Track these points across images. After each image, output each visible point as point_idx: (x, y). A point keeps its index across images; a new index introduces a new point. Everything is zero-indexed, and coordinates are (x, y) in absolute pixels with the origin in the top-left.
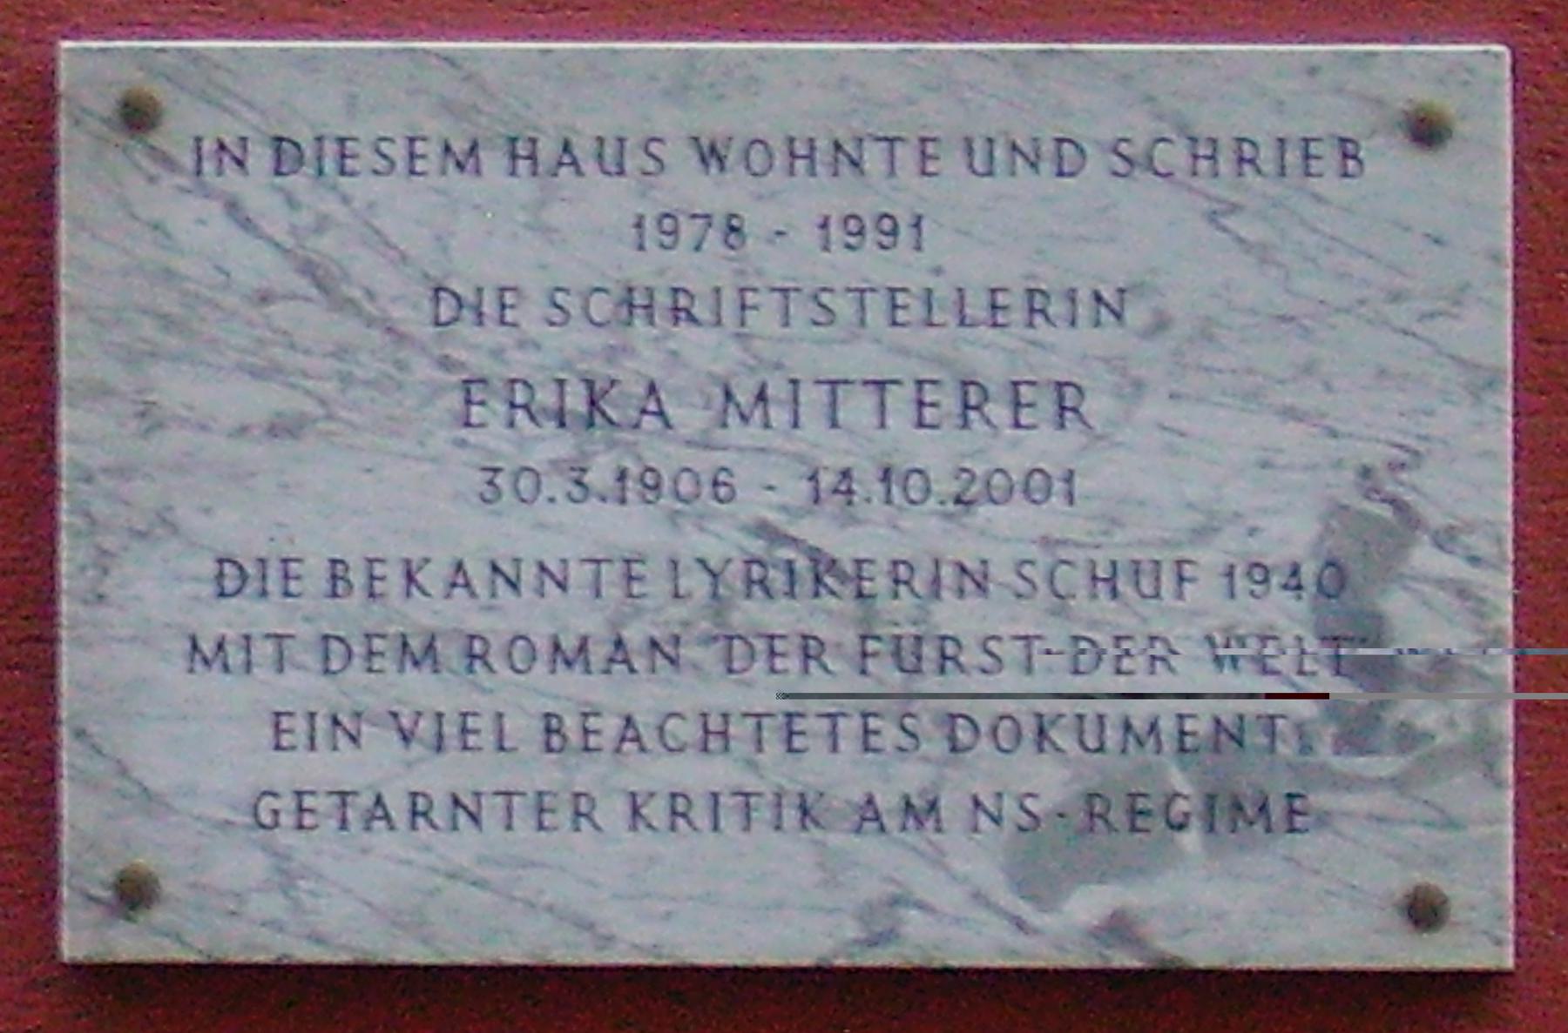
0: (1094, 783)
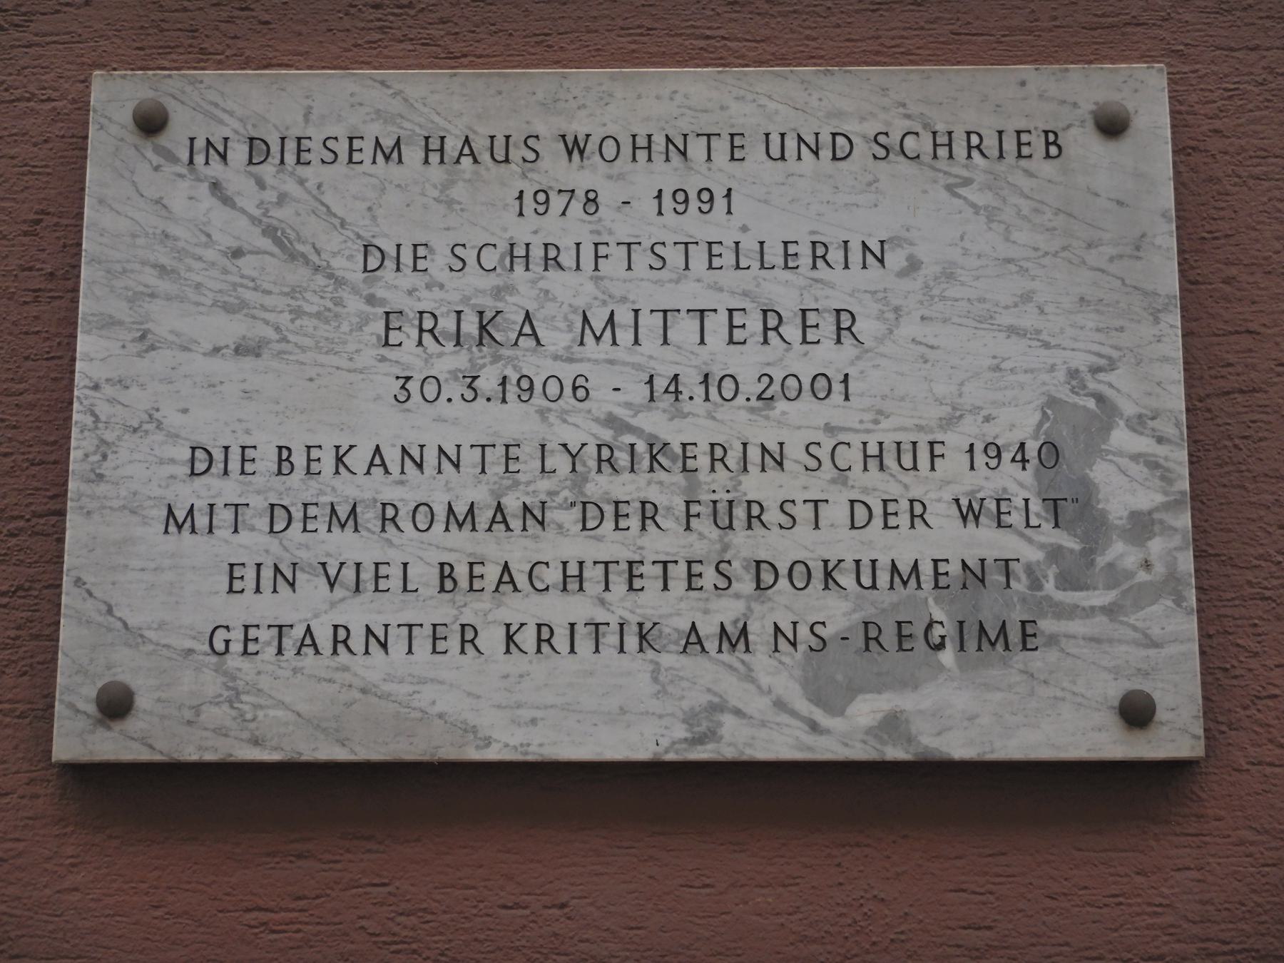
0: (868, 613)
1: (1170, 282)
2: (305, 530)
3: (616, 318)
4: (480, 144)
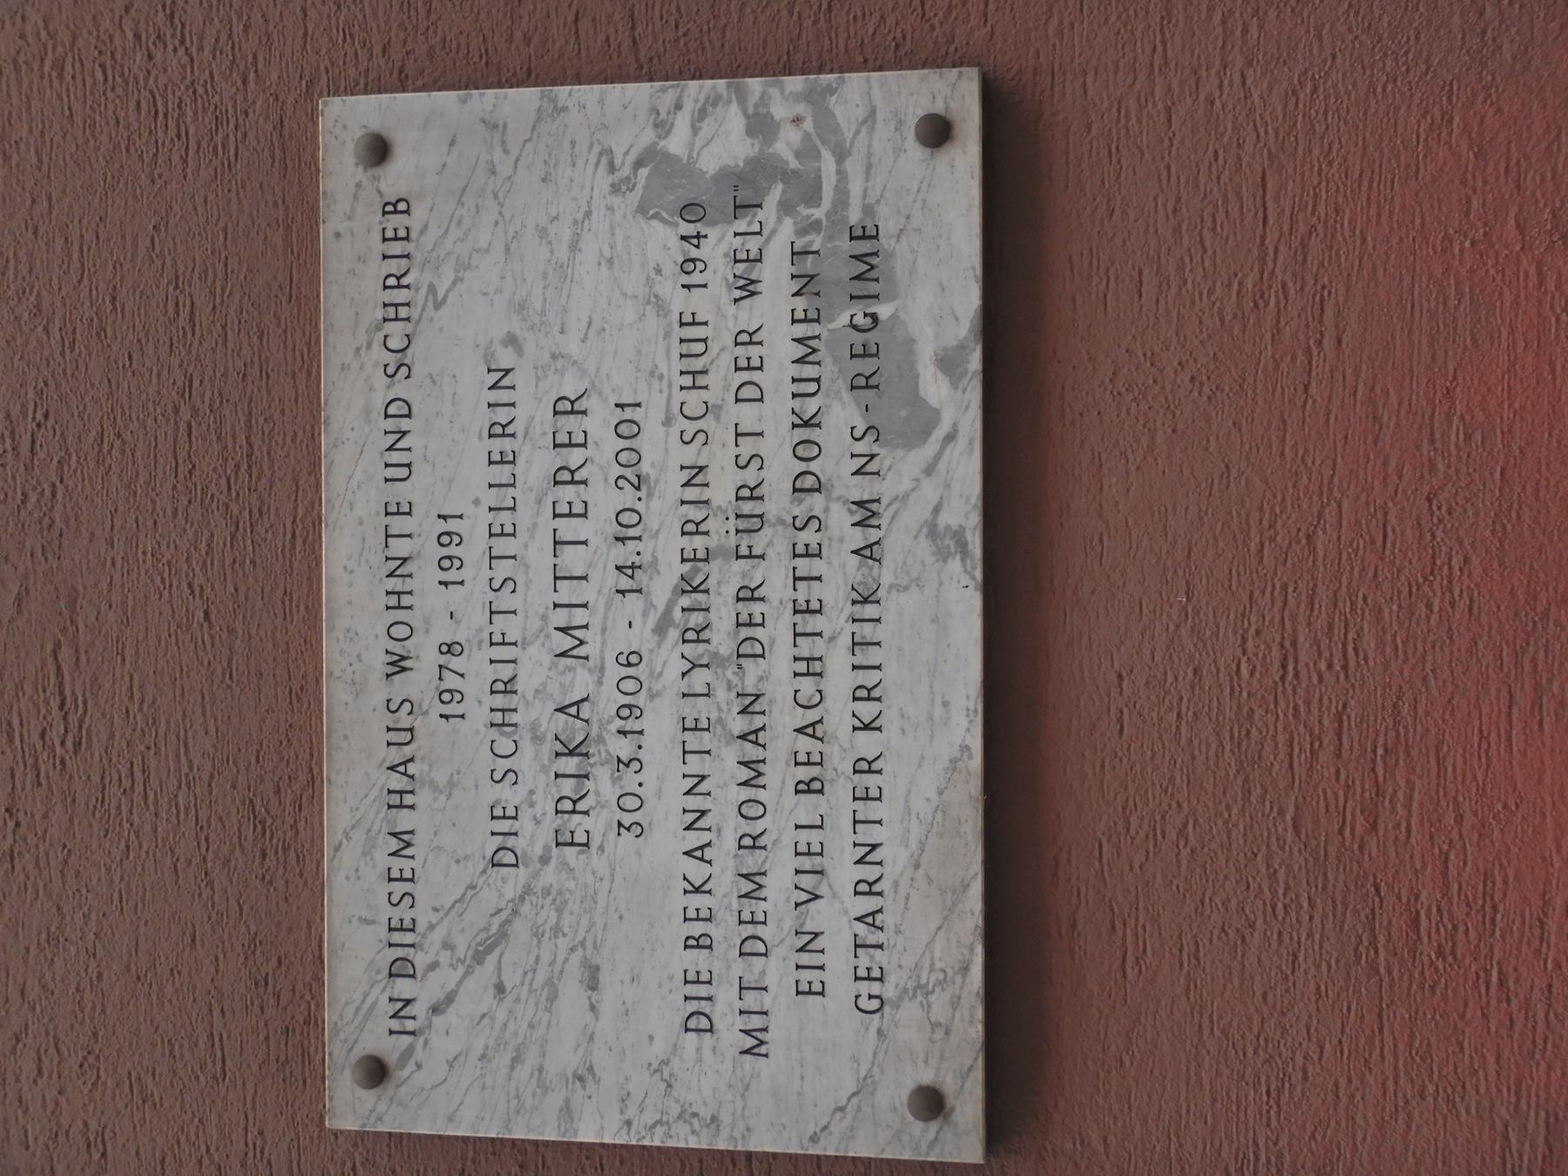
0: (842, 385)
1: (526, 98)
2: (764, 923)
3: (562, 625)
4: (395, 756)
